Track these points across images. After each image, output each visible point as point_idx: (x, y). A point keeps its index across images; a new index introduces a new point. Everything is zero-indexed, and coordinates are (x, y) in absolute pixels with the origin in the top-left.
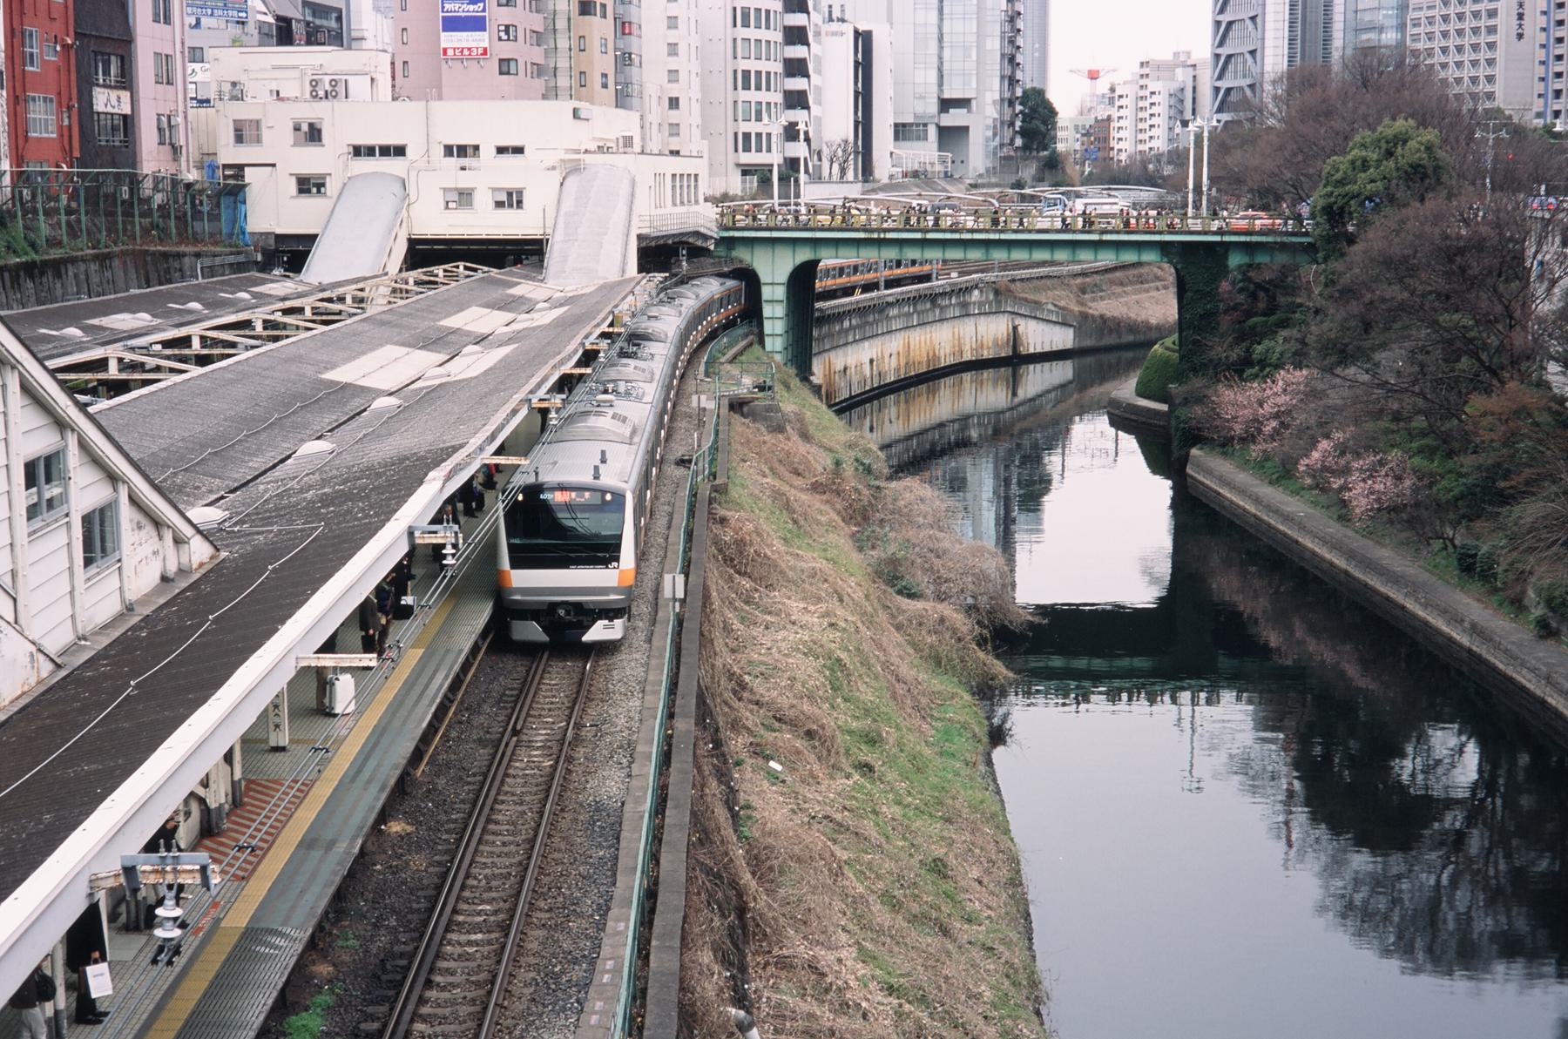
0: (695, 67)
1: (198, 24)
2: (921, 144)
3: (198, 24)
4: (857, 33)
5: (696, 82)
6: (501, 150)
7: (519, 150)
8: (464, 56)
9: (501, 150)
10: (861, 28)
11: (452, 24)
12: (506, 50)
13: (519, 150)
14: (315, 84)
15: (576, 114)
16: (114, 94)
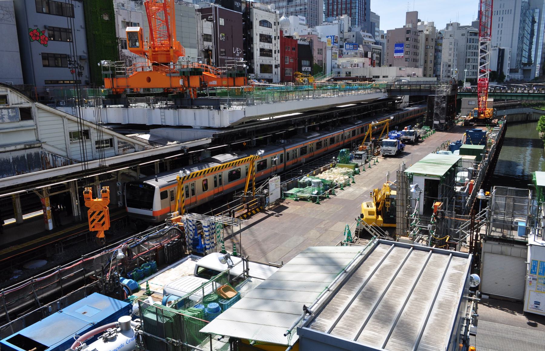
0: (455, 58)
1: (348, 54)
2: (516, 73)
3: (348, 54)
4: (500, 50)
5: (455, 61)
6: (384, 77)
7: (387, 77)
8: (399, 58)
9: (384, 77)
10: (502, 48)
11: (397, 52)
12: (407, 56)
13: (387, 77)
14: (352, 65)
15: (400, 69)
16: (307, 68)
